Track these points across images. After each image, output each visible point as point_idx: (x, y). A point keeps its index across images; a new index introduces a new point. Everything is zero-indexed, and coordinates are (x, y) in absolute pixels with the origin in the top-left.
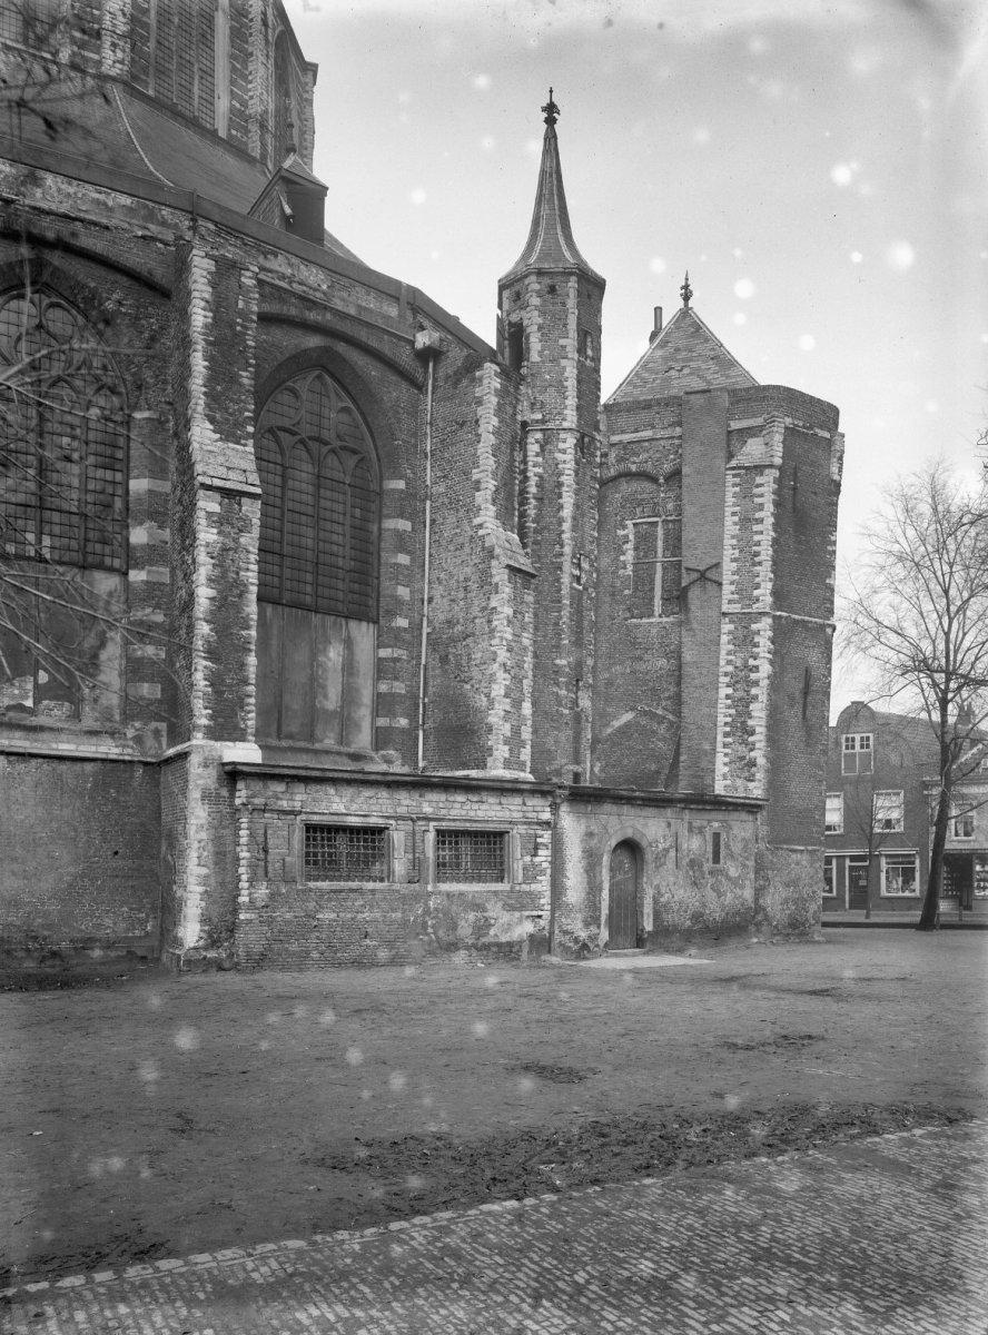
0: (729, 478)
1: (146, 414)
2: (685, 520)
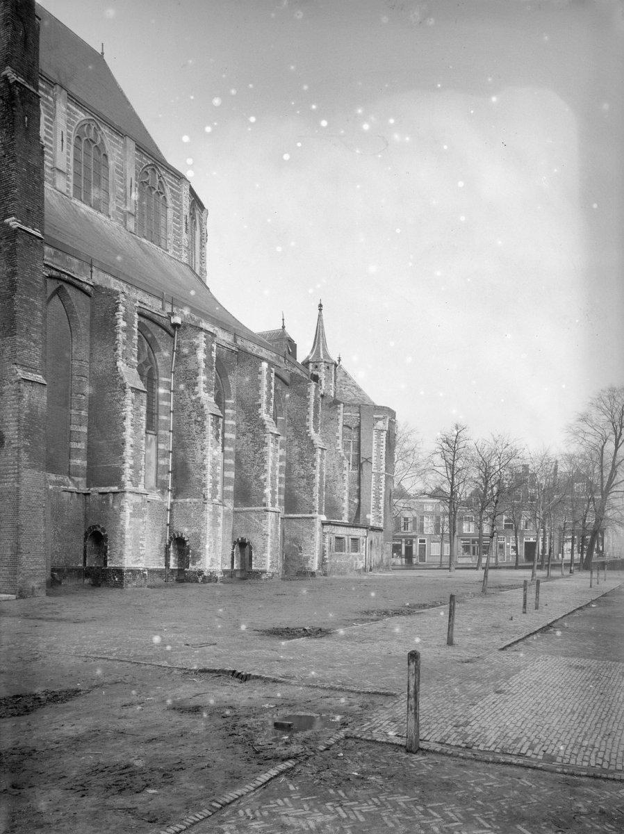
1: (282, 418)
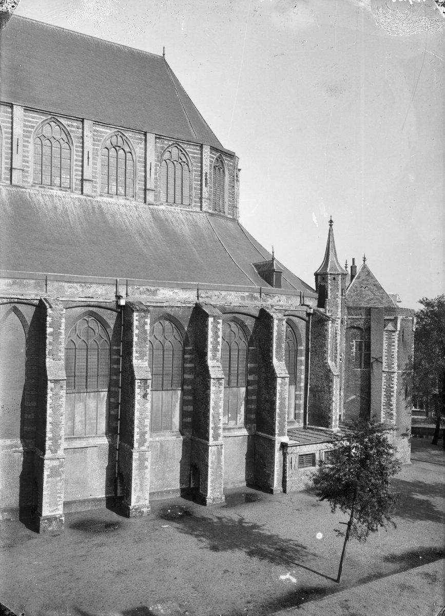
1: (253, 348)
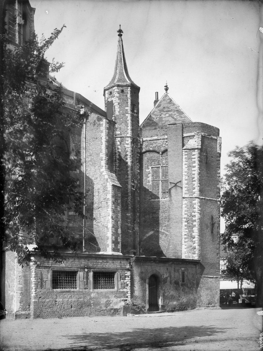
0: (183, 152)
2: (169, 166)
